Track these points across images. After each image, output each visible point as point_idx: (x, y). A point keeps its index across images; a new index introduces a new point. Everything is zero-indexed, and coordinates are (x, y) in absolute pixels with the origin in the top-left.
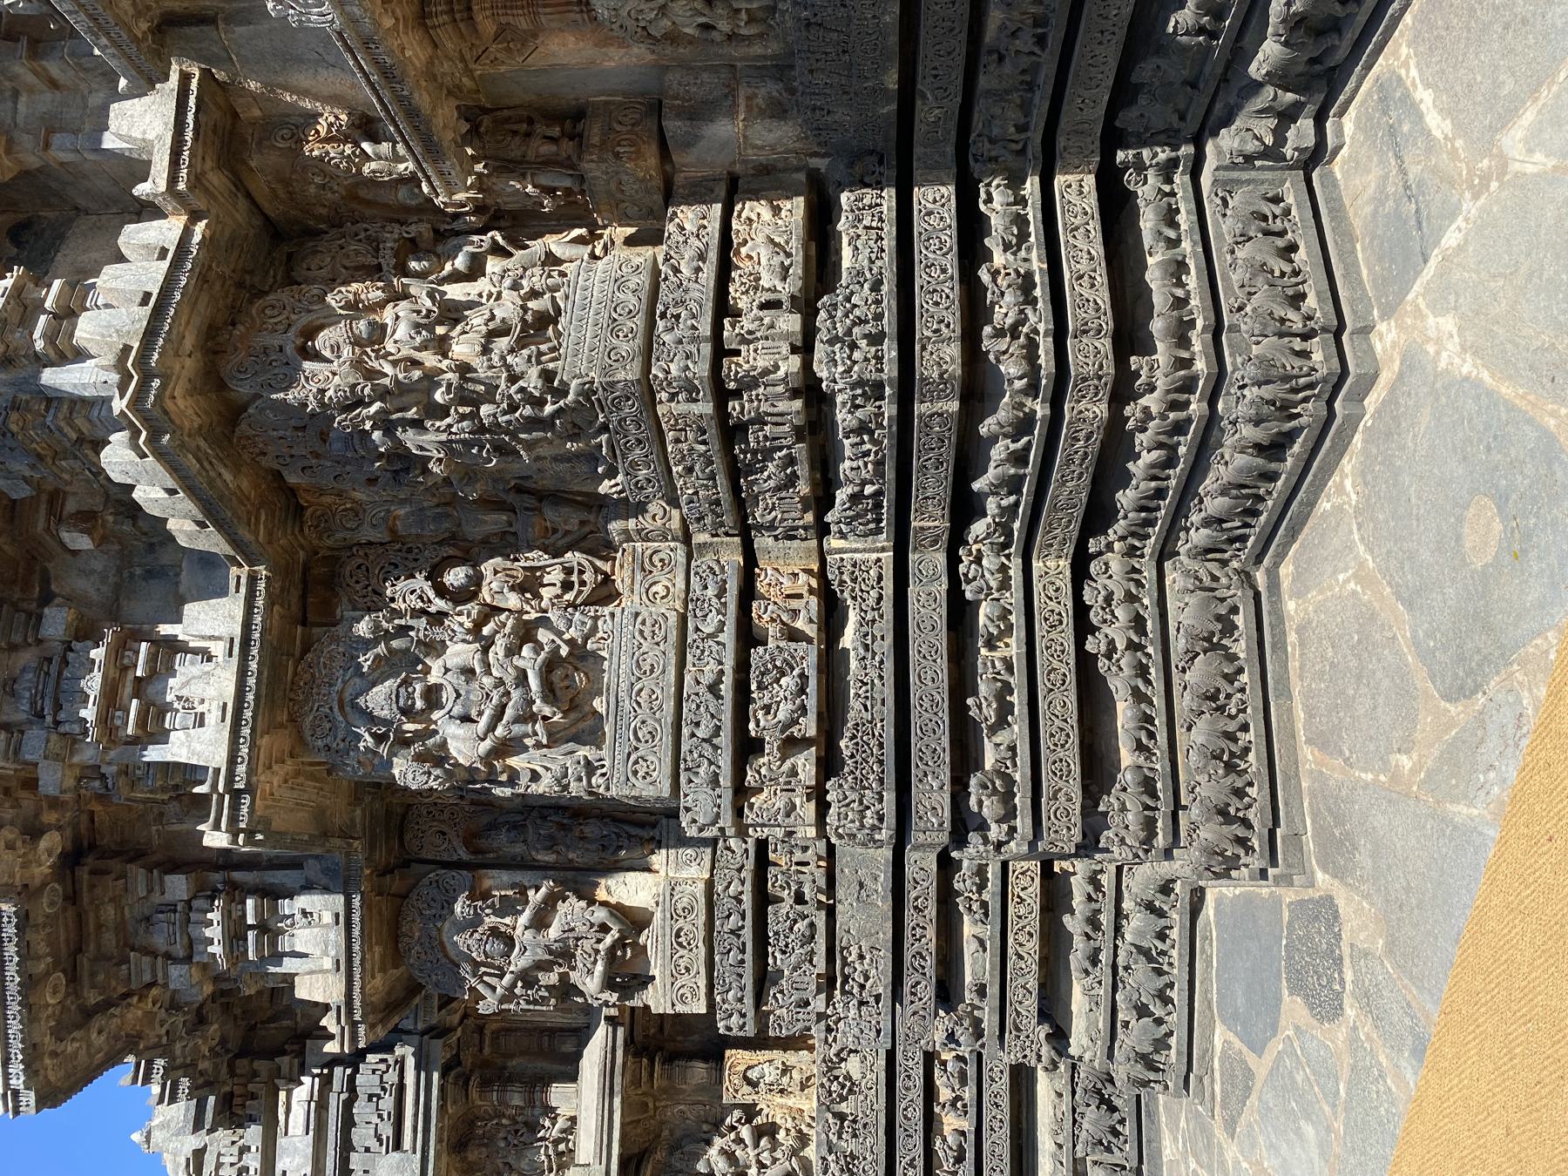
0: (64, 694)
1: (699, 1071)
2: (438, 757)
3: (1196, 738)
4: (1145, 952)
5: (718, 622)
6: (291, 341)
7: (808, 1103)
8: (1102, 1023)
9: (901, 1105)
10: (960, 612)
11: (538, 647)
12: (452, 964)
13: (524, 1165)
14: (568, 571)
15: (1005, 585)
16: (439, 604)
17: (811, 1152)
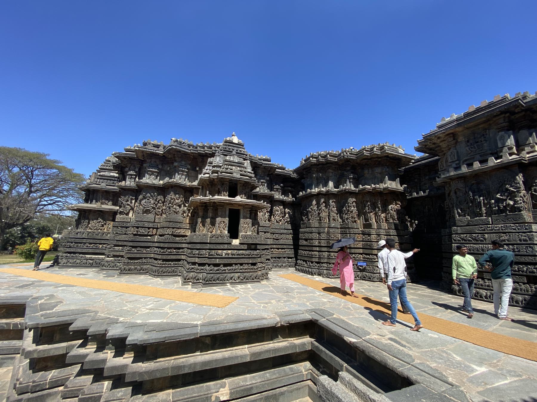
0: (153, 167)
1: (111, 219)
2: (142, 200)
3: (133, 267)
4: (115, 265)
5: (151, 225)
6: (177, 193)
7: (105, 231)
8: (108, 261)
9: (103, 241)
10: (148, 247)
11: (151, 209)
12: (125, 196)
13: (103, 199)
14: (160, 212)
15: (150, 251)
16: (158, 200)
17: (100, 231)
